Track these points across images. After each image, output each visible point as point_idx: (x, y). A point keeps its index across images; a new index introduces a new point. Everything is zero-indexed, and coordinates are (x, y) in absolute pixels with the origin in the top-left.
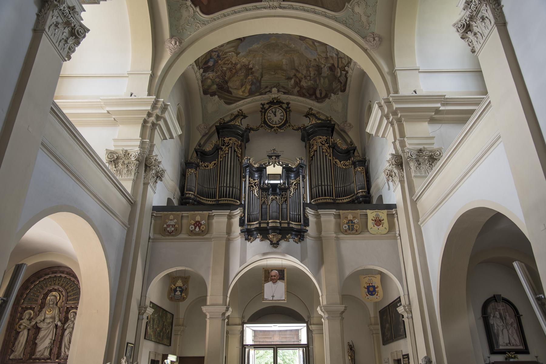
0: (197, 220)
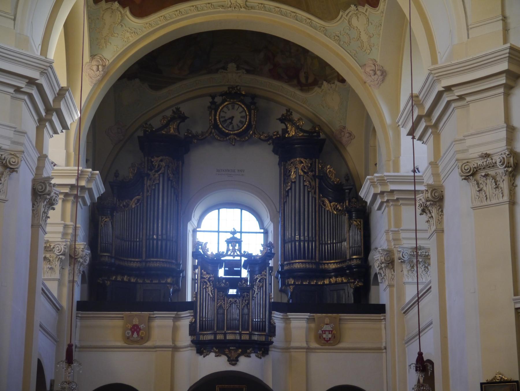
0: (134, 323)
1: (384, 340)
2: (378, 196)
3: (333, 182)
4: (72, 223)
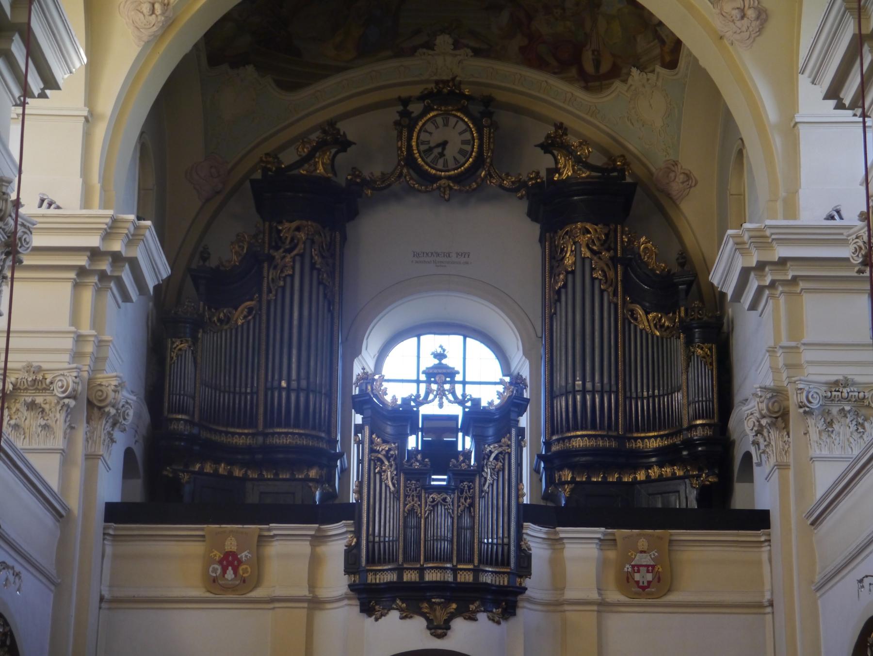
1: (767, 586)
2: (752, 275)
3: (653, 270)
4: (93, 332)
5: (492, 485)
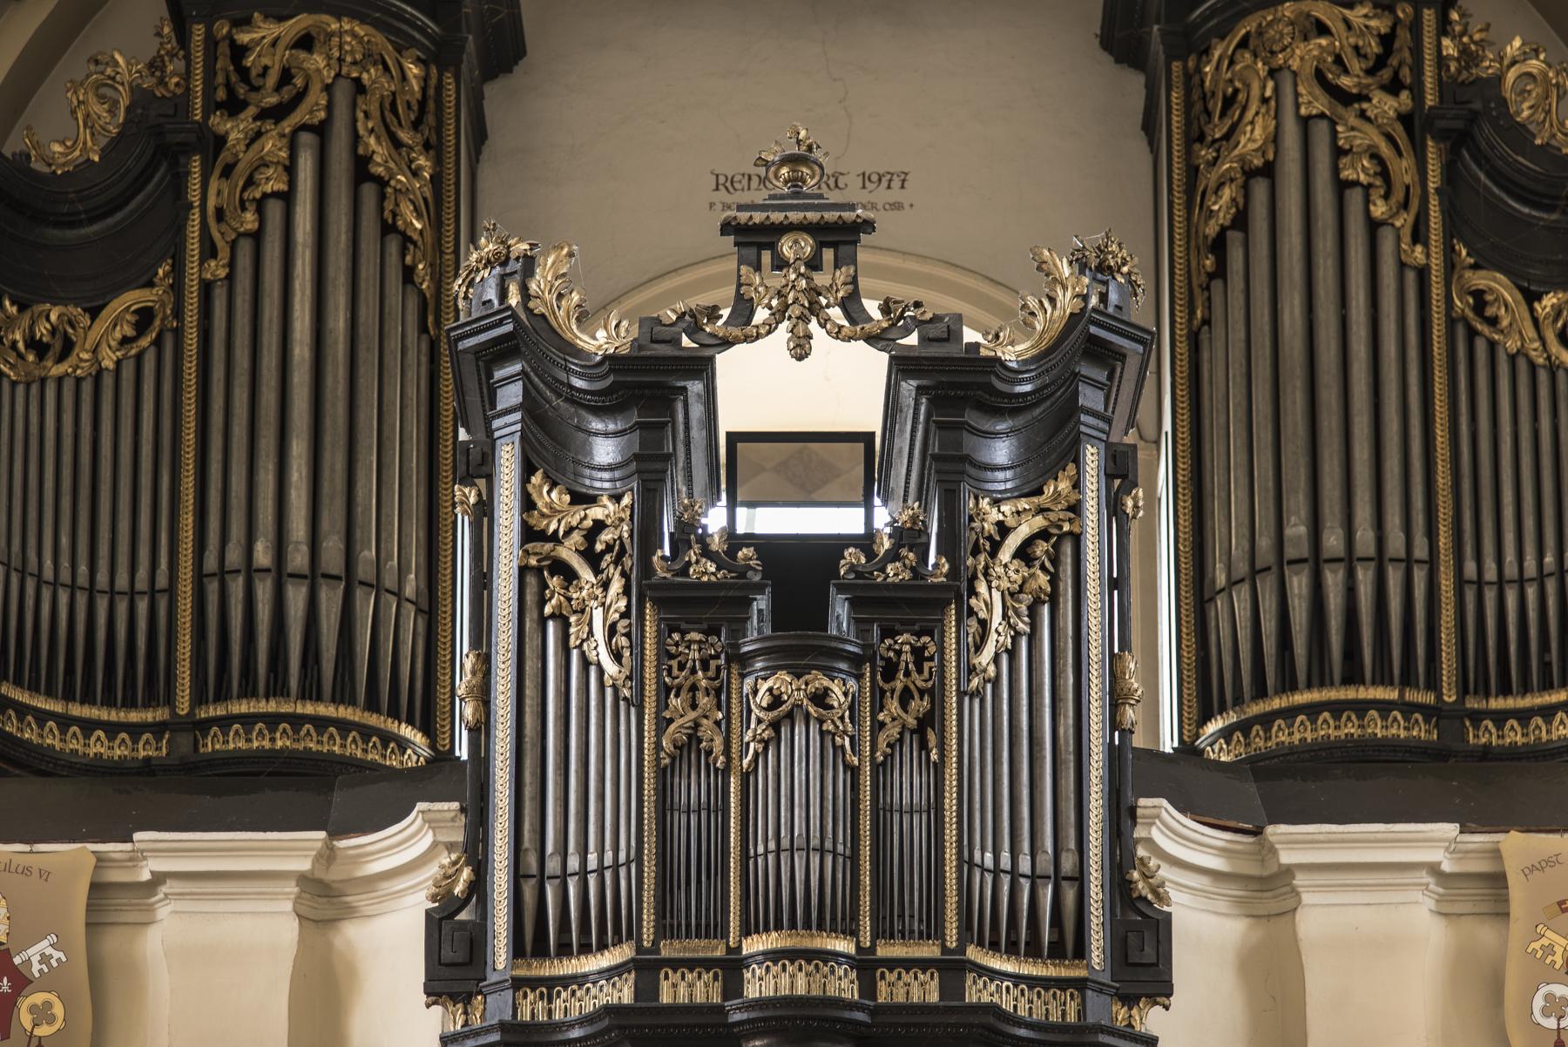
5: (1012, 653)
